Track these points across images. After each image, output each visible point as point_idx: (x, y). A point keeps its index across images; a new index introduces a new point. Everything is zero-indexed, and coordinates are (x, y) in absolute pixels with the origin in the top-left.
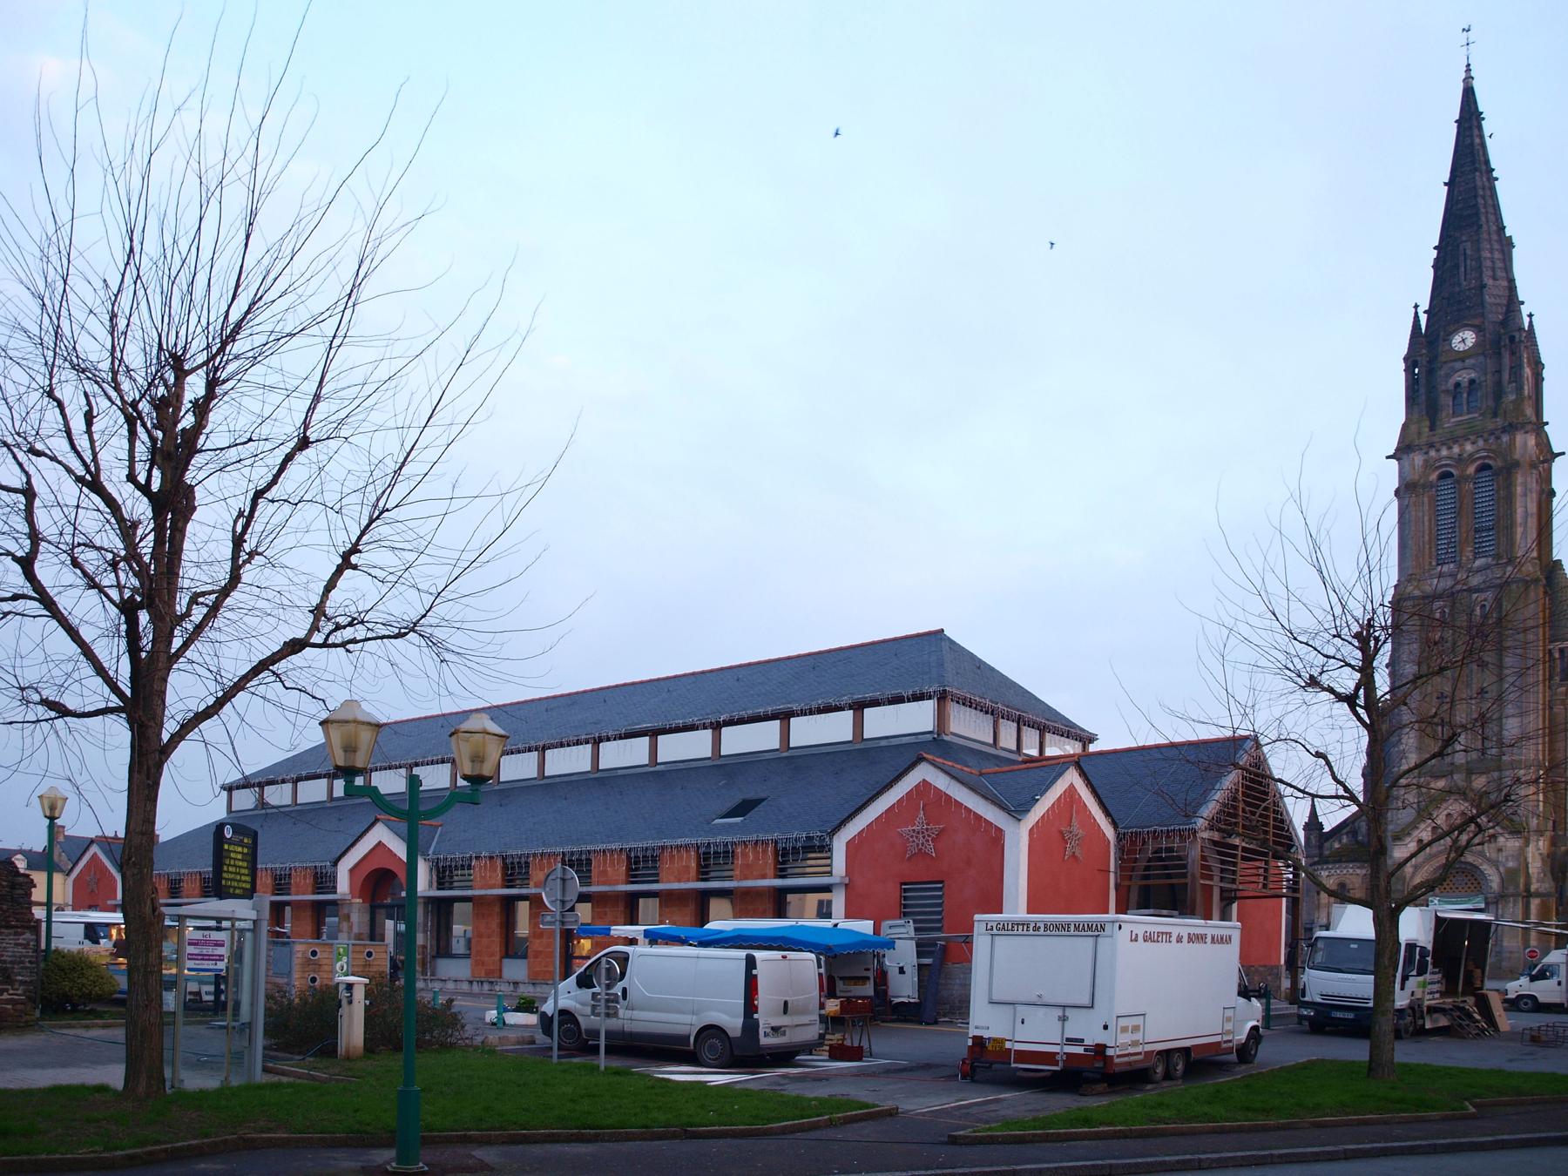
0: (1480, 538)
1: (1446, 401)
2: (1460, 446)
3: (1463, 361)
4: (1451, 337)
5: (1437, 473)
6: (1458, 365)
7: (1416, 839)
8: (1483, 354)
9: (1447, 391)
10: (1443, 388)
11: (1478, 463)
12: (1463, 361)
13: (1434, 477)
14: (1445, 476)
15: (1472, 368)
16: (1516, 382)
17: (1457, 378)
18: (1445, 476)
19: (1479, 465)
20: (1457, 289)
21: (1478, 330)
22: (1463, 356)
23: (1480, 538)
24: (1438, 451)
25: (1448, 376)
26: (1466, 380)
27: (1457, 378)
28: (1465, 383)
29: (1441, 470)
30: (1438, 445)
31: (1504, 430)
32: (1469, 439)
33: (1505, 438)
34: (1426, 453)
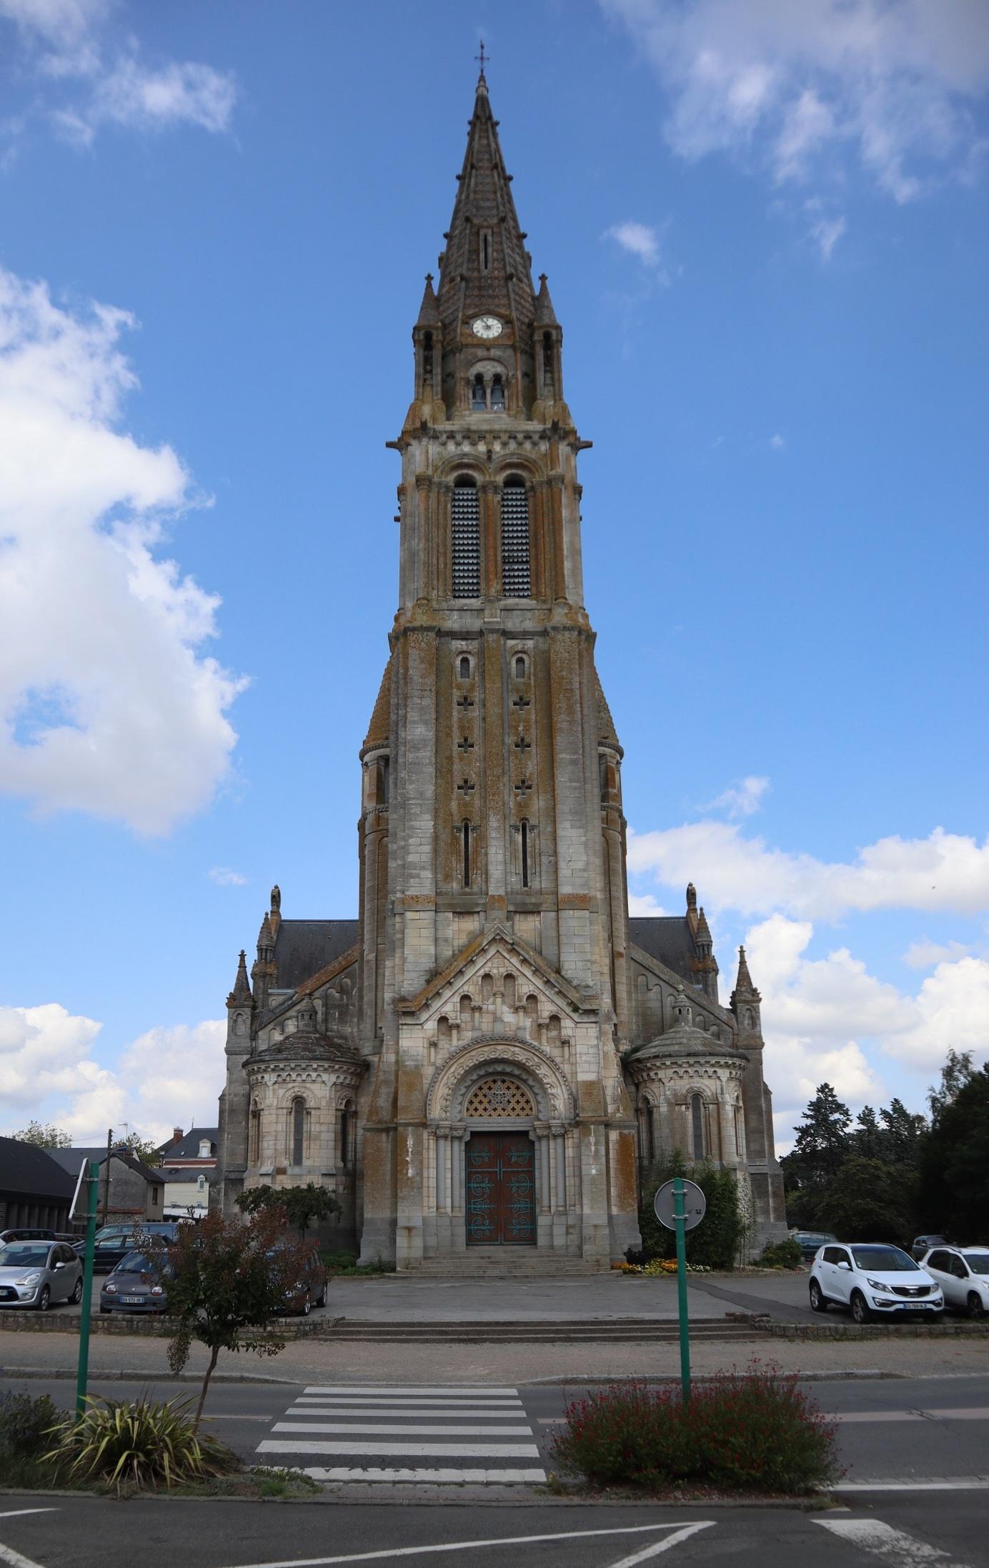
0: (509, 570)
1: (464, 391)
2: (486, 444)
3: (488, 349)
4: (471, 322)
5: (455, 474)
6: (481, 353)
7: (437, 1016)
8: (513, 347)
9: (468, 381)
10: (463, 375)
11: (509, 472)
12: (488, 349)
13: (451, 478)
14: (464, 482)
15: (498, 360)
16: (553, 385)
17: (479, 368)
18: (464, 482)
19: (508, 476)
20: (475, 274)
21: (507, 321)
22: (486, 345)
23: (509, 570)
24: (458, 444)
25: (471, 364)
26: (490, 372)
27: (479, 368)
28: (488, 377)
29: (460, 472)
30: (459, 437)
31: (543, 436)
32: (499, 437)
33: (544, 447)
34: (444, 444)
